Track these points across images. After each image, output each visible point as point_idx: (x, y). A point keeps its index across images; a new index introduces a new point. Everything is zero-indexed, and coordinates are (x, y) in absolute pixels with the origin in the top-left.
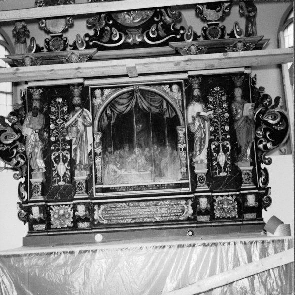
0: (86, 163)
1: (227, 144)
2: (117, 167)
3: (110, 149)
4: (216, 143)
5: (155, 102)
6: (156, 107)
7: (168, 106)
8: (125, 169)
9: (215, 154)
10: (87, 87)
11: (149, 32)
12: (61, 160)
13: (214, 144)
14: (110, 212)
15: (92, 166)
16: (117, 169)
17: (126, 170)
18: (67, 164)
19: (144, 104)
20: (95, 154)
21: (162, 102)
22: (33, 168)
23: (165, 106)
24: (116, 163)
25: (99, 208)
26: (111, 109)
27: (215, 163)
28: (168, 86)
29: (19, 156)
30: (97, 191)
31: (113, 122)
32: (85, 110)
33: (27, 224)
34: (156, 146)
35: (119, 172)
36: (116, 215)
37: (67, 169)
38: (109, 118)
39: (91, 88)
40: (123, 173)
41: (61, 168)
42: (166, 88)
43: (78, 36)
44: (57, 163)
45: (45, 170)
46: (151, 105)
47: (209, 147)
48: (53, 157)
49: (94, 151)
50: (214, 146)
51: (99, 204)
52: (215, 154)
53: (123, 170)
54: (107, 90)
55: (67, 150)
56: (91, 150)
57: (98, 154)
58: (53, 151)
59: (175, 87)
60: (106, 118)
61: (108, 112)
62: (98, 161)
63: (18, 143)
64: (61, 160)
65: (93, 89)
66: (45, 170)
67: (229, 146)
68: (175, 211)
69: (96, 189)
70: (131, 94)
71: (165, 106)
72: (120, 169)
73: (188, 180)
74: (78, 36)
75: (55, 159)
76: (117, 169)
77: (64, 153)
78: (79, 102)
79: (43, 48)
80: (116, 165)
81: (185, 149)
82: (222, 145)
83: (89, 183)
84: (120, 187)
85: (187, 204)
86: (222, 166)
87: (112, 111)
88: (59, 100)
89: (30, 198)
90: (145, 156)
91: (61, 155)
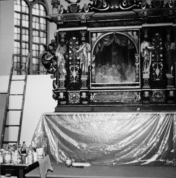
0: (87, 71)
1: (161, 64)
2: (103, 74)
3: (99, 65)
4: (155, 63)
6: (124, 43)
7: (130, 43)
9: (154, 69)
10: (89, 31)
11: (122, 3)
12: (74, 69)
13: (154, 64)
14: (99, 97)
15: (90, 73)
16: (103, 75)
17: (107, 76)
18: (77, 72)
19: (118, 42)
20: (92, 67)
22: (60, 73)
23: (129, 43)
25: (93, 95)
26: (100, 43)
27: (154, 74)
28: (131, 32)
29: (54, 67)
30: (92, 86)
32: (87, 44)
33: (57, 101)
34: (123, 64)
35: (104, 77)
36: (102, 98)
37: (77, 74)
38: (100, 48)
39: (91, 32)
40: (106, 77)
41: (74, 74)
42: (130, 33)
43: (85, 4)
44: (73, 71)
45: (66, 74)
47: (151, 65)
48: (70, 68)
49: (91, 65)
50: (154, 65)
51: (93, 93)
52: (154, 69)
53: (106, 76)
54: (99, 33)
58: (70, 65)
59: (135, 33)
60: (98, 48)
61: (99, 45)
62: (93, 70)
63: (53, 60)
64: (74, 69)
65: (92, 33)
66: (66, 74)
67: (162, 65)
68: (132, 98)
69: (92, 85)
70: (111, 36)
71: (129, 43)
72: (104, 75)
73: (139, 82)
74: (85, 4)
75: (71, 69)
76: (103, 75)
77: (76, 66)
78: (84, 39)
79: (67, 11)
80: (102, 73)
81: (138, 66)
82: (158, 64)
83: (88, 81)
84: (104, 85)
85: (138, 94)
86: (158, 75)
87: (101, 45)
88: (74, 38)
89: (59, 88)
90: (118, 69)
91: (74, 67)
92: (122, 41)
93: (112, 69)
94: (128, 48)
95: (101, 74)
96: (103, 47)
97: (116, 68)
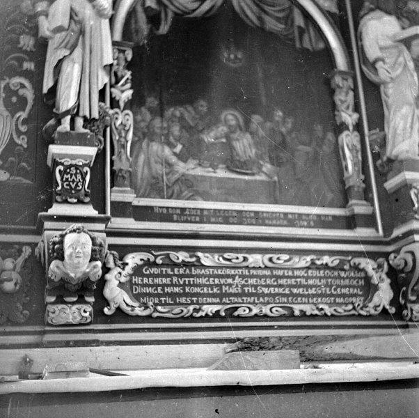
2: (175, 154)
5: (273, 6)
6: (278, 19)
7: (307, 25)
8: (196, 162)
14: (157, 281)
16: (174, 159)
21: (291, 11)
24: (172, 139)
31: (164, 29)
35: (181, 167)
36: (177, 290)
37: (19, 133)
40: (192, 172)
46: (266, 12)
51: (123, 251)
53: (192, 163)
55: (26, 74)
56: (105, 85)
57: (122, 105)
68: (345, 291)
71: (299, 21)
80: (171, 146)
81: (358, 127)
84: (183, 210)
92: (266, 8)
93: (225, 129)
94: (298, 45)
95: (167, 151)
96: (170, 15)
97: (246, 127)
